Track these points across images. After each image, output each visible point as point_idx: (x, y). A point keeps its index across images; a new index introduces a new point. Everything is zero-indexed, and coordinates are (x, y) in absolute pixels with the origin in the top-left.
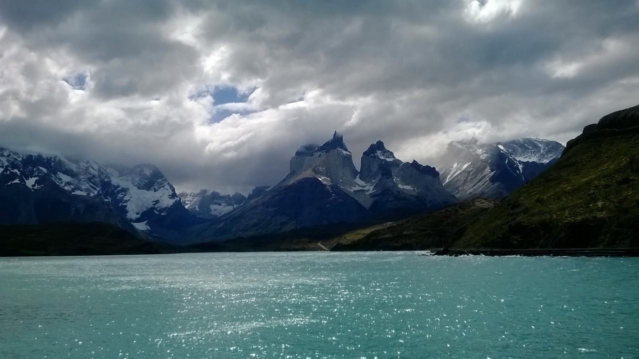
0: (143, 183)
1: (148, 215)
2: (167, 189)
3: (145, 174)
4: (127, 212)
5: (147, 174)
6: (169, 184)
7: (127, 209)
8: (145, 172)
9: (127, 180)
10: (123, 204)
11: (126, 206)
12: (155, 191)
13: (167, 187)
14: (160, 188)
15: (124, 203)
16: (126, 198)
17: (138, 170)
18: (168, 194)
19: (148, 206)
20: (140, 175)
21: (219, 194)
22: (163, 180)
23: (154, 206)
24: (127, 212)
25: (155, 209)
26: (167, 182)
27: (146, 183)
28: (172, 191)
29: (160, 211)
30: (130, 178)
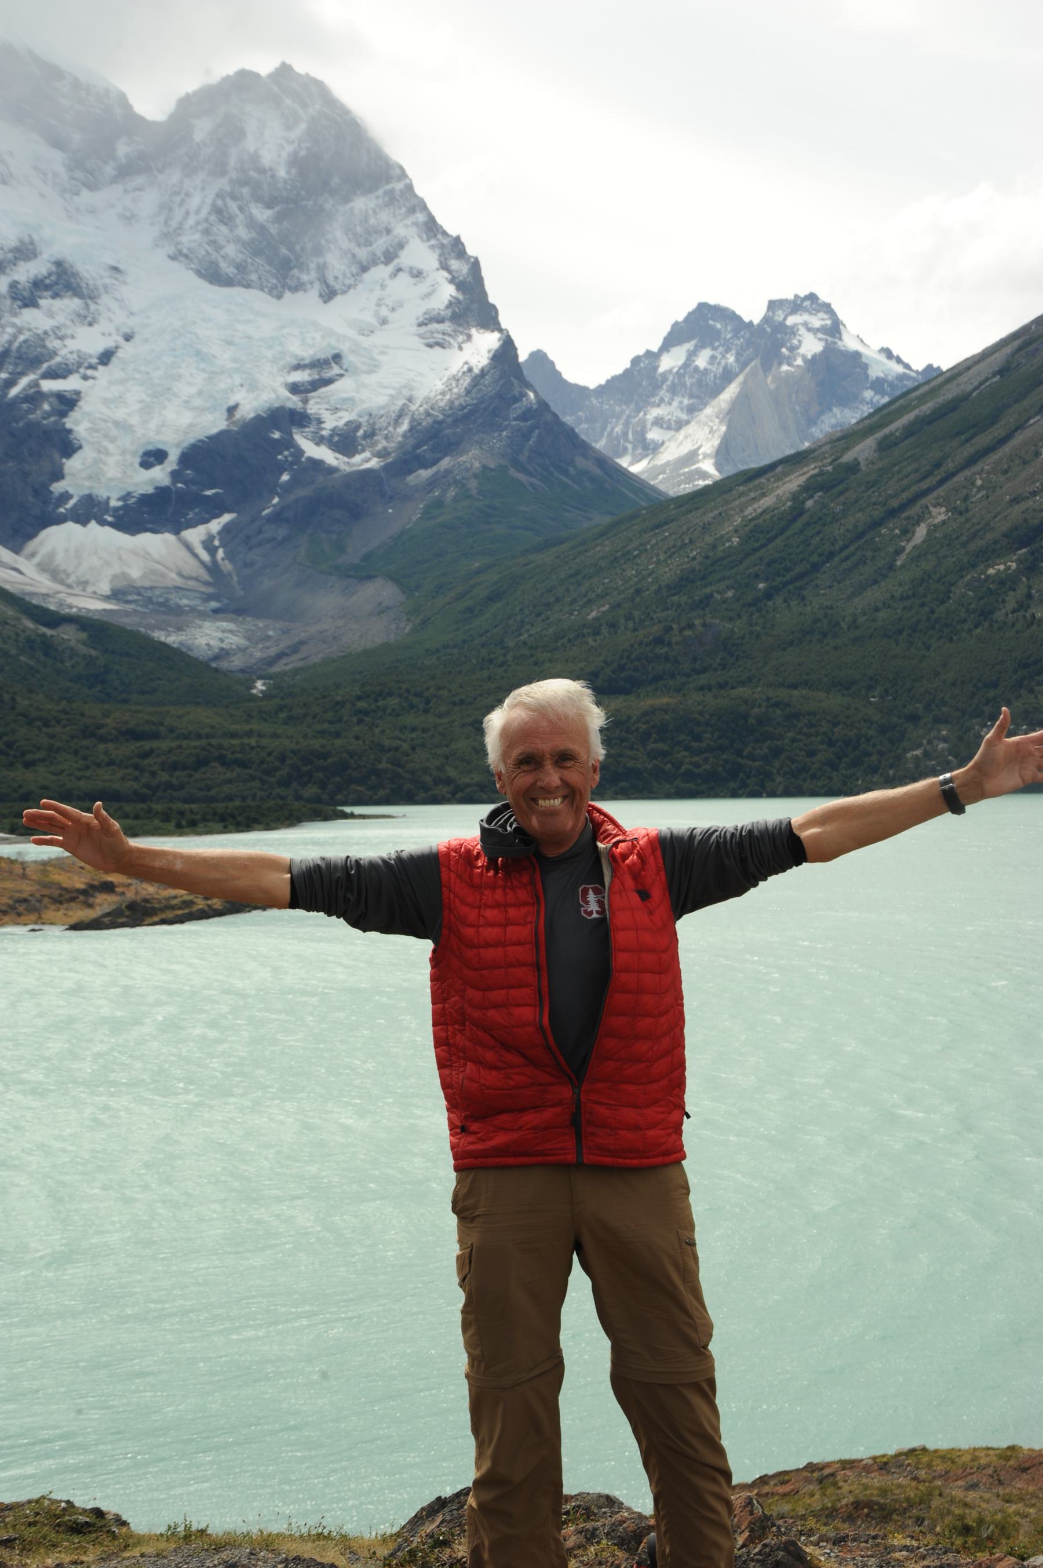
0: (242, 232)
1: (234, 472)
2: (417, 274)
3: (255, 158)
4: (69, 447)
5: (267, 158)
6: (431, 227)
7: (69, 423)
8: (250, 144)
9: (129, 218)
10: (48, 386)
11: (68, 402)
12: (329, 294)
13: (420, 254)
14: (364, 269)
15: (52, 375)
16: (88, 342)
17: (202, 130)
18: (416, 310)
19: (239, 397)
20: (220, 169)
21: (865, 367)
22: (391, 199)
23: (294, 402)
24: (69, 447)
25: (299, 419)
26: (421, 217)
27: (262, 229)
28: (460, 286)
29: (345, 441)
30: (148, 201)
